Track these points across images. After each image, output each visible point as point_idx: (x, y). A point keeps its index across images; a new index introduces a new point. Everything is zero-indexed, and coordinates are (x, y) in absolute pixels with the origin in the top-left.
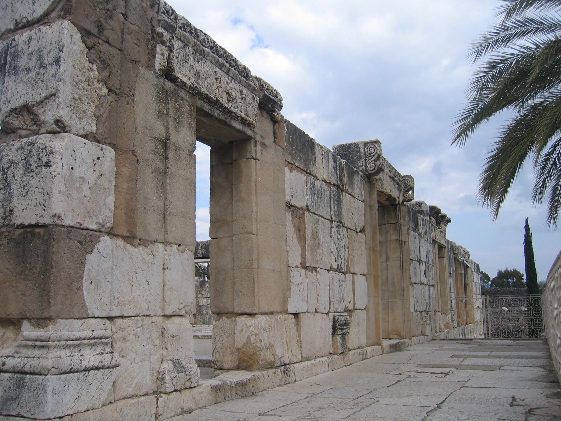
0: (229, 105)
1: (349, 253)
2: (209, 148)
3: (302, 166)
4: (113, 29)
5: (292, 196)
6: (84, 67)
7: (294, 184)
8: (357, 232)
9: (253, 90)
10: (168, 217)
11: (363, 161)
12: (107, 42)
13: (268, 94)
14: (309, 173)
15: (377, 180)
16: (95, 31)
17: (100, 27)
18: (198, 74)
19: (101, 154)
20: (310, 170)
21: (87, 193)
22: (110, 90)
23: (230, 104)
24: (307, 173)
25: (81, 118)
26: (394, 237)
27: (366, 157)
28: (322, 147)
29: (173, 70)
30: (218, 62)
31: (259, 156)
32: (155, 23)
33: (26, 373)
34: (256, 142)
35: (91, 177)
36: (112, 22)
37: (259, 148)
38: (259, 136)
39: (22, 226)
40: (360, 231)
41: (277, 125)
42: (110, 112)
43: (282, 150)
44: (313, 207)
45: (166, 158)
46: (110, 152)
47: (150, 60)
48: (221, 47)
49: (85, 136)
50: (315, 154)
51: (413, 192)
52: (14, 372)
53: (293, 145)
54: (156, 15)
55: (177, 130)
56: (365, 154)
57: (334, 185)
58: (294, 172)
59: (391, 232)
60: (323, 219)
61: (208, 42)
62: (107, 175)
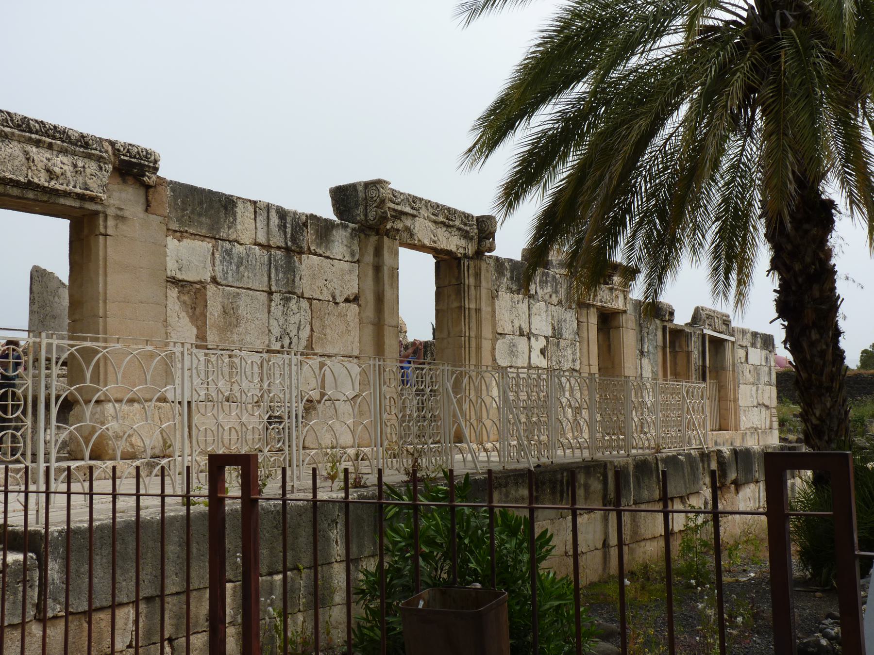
1: (312, 330)
2: (66, 223)
3: (204, 232)
5: (180, 270)
7: (189, 255)
8: (336, 303)
9: (99, 159)
11: (361, 209)
13: (126, 158)
14: (219, 239)
15: (398, 230)
20: (223, 234)
23: (53, 183)
24: (215, 239)
26: (455, 304)
27: (367, 202)
28: (255, 203)
30: (30, 139)
31: (109, 232)
34: (106, 216)
37: (111, 223)
38: (113, 209)
40: (347, 300)
41: (151, 190)
43: (161, 219)
44: (226, 279)
48: (36, 121)
50: (234, 214)
51: (494, 240)
53: (183, 210)
56: (366, 199)
57: (279, 248)
58: (186, 242)
59: (453, 297)
60: (251, 292)
61: (12, 121)
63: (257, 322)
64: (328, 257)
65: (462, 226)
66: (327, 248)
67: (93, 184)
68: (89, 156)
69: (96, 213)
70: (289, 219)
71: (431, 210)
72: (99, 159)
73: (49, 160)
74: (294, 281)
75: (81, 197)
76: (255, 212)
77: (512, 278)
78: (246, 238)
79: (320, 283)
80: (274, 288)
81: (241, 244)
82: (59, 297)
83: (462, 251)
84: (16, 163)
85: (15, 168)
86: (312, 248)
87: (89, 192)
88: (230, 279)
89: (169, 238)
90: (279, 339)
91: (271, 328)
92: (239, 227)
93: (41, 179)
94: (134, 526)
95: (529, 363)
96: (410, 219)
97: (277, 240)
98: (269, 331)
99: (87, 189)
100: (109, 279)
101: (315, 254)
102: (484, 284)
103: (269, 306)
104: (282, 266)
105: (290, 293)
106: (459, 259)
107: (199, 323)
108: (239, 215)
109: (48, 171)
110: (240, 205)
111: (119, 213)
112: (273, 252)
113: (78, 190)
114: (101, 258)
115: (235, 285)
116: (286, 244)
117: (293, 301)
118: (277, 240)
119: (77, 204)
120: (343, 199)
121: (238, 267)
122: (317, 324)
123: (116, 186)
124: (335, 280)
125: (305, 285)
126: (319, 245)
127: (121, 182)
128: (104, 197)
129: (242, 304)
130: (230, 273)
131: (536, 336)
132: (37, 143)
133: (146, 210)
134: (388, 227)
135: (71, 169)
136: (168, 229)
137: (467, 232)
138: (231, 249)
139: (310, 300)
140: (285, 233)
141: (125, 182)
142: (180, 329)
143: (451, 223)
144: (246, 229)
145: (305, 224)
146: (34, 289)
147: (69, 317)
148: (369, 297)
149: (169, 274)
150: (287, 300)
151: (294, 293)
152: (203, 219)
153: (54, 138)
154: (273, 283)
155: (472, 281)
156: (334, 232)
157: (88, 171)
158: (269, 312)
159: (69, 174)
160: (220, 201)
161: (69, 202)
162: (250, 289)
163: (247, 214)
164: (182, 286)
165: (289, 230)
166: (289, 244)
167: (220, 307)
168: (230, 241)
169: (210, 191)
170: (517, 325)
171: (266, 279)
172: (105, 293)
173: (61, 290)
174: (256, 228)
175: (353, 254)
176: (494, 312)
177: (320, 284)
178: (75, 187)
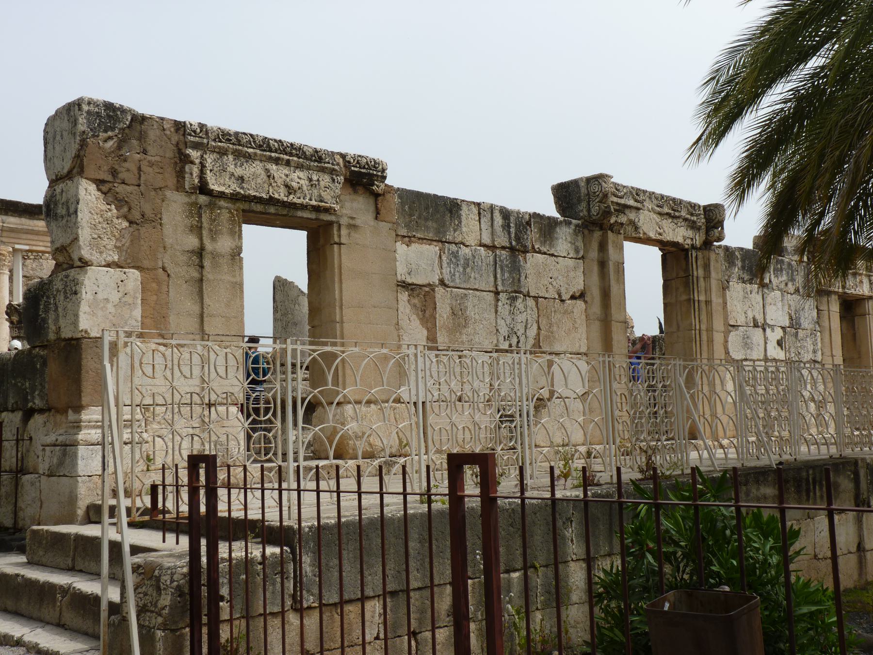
0: (292, 199)
1: (539, 328)
2: (303, 234)
3: (431, 235)
4: (128, 170)
5: (409, 274)
6: (102, 211)
7: (417, 259)
8: (563, 301)
9: (332, 172)
10: (205, 319)
12: (123, 183)
13: (356, 169)
15: (622, 224)
16: (109, 178)
17: (114, 173)
18: (241, 179)
19: (124, 277)
20: (449, 237)
21: (113, 310)
22: (131, 223)
23: (291, 197)
24: (442, 242)
25: (101, 253)
26: (684, 297)
28: (479, 204)
29: (207, 184)
30: (271, 157)
31: (343, 240)
32: (182, 146)
33: (67, 445)
34: (340, 226)
35: (115, 297)
36: (126, 165)
37: (344, 232)
38: (346, 218)
39: (65, 340)
40: (573, 297)
41: (380, 198)
42: (132, 241)
43: (390, 225)
44: (453, 281)
45: (202, 267)
46: (134, 274)
47: (178, 181)
48: (275, 141)
49: (108, 265)
50: (459, 217)
51: (723, 228)
52: (62, 446)
53: (411, 215)
54: (182, 137)
55: (213, 239)
56: (588, 194)
57: (503, 248)
58: (415, 246)
59: (681, 289)
60: (478, 293)
61: (254, 142)
62: (132, 293)
63: (484, 322)
64: (553, 255)
65: (689, 216)
66: (551, 246)
67: (326, 196)
68: (323, 170)
69: (331, 223)
70: (512, 219)
71: (655, 202)
72: (332, 172)
73: (287, 176)
74: (519, 280)
75: (316, 209)
76: (479, 214)
77: (743, 268)
78: (472, 240)
79: (545, 281)
80: (500, 288)
81: (467, 246)
82: (299, 305)
83: (689, 242)
84: (259, 181)
85: (258, 186)
86: (536, 247)
87: (323, 204)
88: (458, 281)
89: (398, 244)
90: (507, 338)
91: (499, 328)
92: (464, 229)
93: (281, 194)
94: (426, 519)
95: (766, 355)
96: (634, 211)
97: (502, 240)
98: (497, 330)
99: (321, 201)
100: (344, 285)
101: (540, 252)
102: (713, 274)
103: (496, 306)
104: (507, 266)
105: (516, 292)
106: (687, 250)
107: (429, 324)
108: (463, 218)
109: (287, 186)
110: (464, 207)
111: (352, 222)
112: (498, 252)
113: (314, 203)
114: (336, 266)
115: (462, 286)
116: (511, 243)
117: (520, 300)
118: (502, 240)
119: (313, 216)
120: (565, 197)
121: (464, 269)
122: (544, 322)
123: (348, 197)
124: (560, 277)
125: (531, 284)
126: (543, 243)
127: (352, 192)
128: (337, 207)
129: (469, 304)
130: (457, 274)
131: (772, 327)
132: (277, 161)
133: (376, 218)
134: (612, 221)
135: (307, 182)
136: (397, 235)
137: (694, 222)
138: (458, 252)
139: (536, 298)
140: (509, 233)
141: (355, 192)
142: (412, 332)
143: (677, 214)
144: (471, 230)
145: (528, 223)
146: (277, 298)
147: (309, 324)
148: (595, 293)
149: (399, 279)
150: (514, 299)
151: (520, 292)
152: (430, 223)
153: (291, 155)
154: (499, 283)
155: (701, 272)
156: (558, 229)
157: (322, 183)
158: (496, 312)
159: (305, 188)
160: (445, 204)
161: (306, 214)
162: (477, 290)
163: (472, 216)
164: (412, 289)
165: (513, 230)
166: (514, 243)
167: (448, 309)
168: (456, 244)
169: (435, 195)
170: (750, 315)
171: (492, 279)
172: (341, 300)
173: (301, 298)
174: (480, 229)
175: (577, 251)
176: (725, 303)
177: (546, 282)
178: (311, 200)
